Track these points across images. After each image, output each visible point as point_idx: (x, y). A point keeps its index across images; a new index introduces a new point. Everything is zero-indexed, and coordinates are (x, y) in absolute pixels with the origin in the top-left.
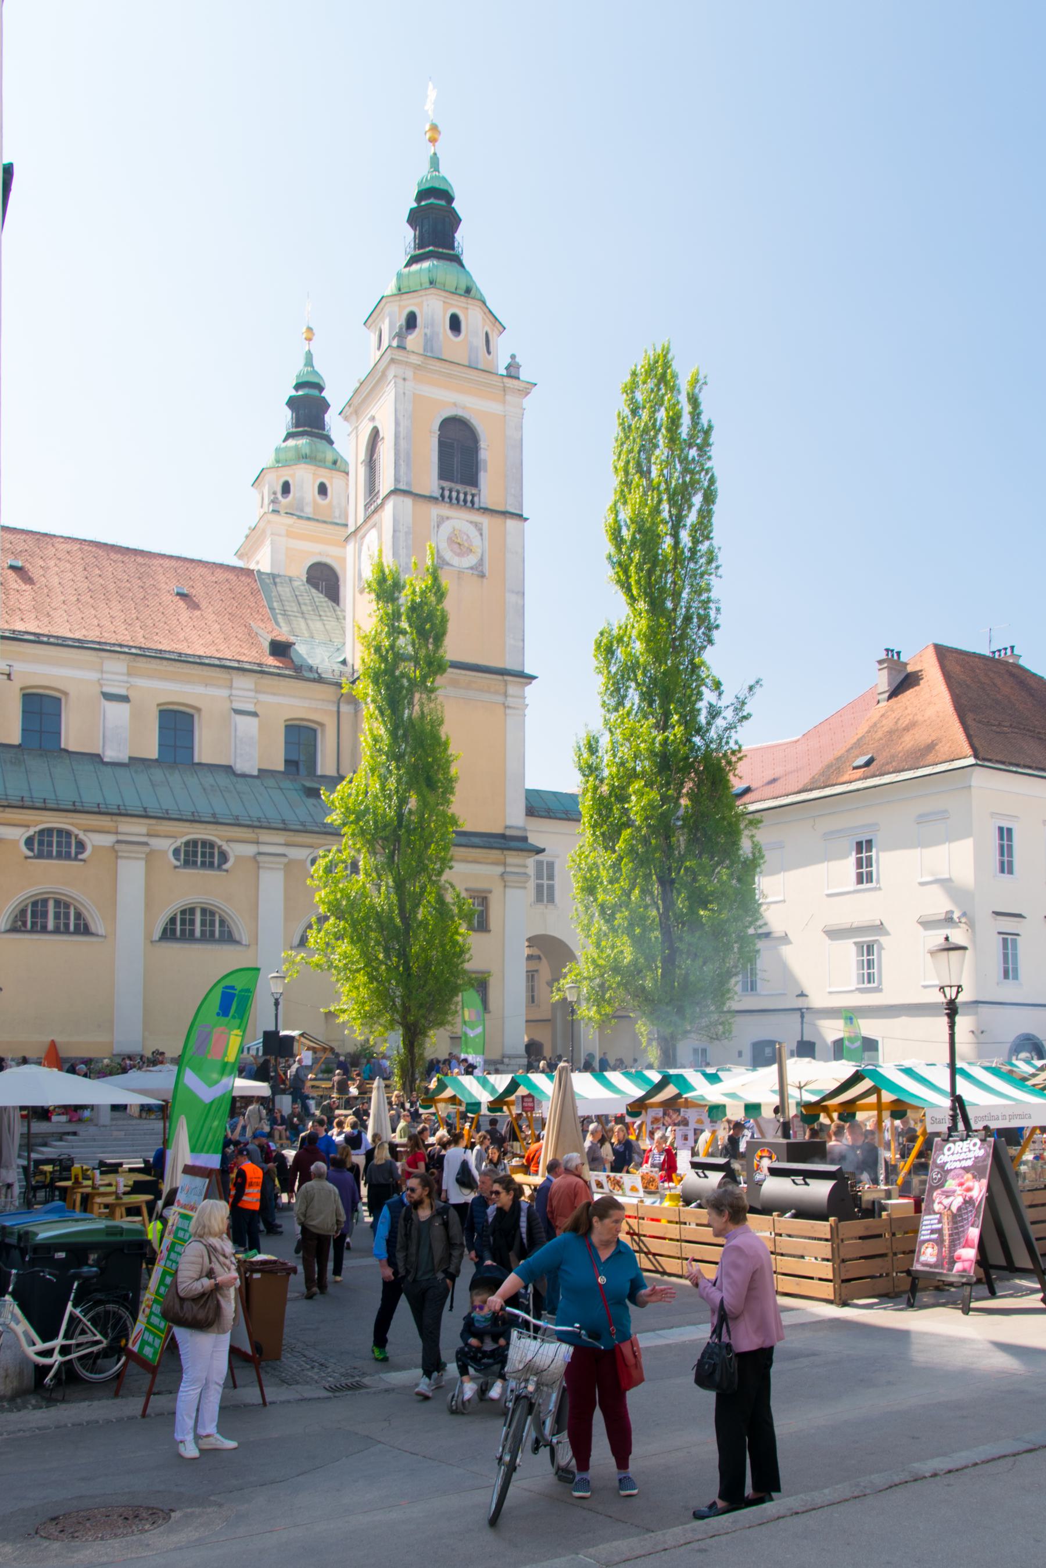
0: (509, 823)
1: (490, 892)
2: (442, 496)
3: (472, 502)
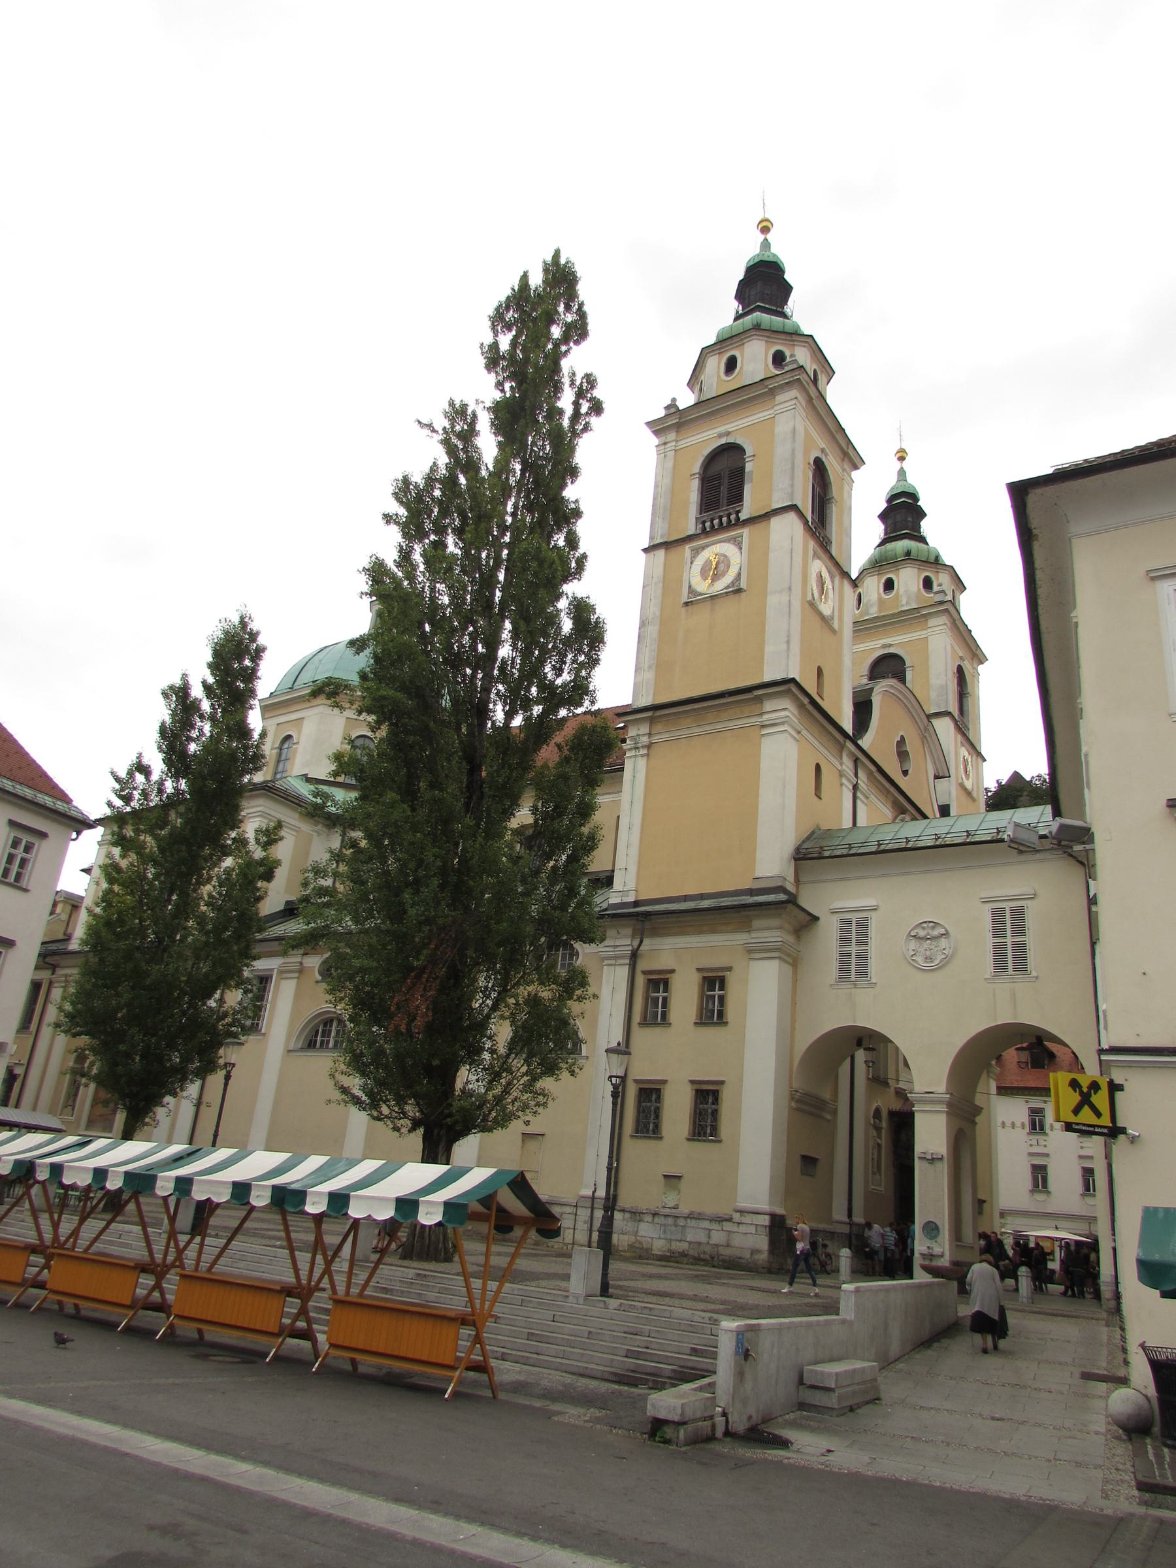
0: (758, 875)
1: (730, 969)
2: (704, 529)
3: (738, 519)
